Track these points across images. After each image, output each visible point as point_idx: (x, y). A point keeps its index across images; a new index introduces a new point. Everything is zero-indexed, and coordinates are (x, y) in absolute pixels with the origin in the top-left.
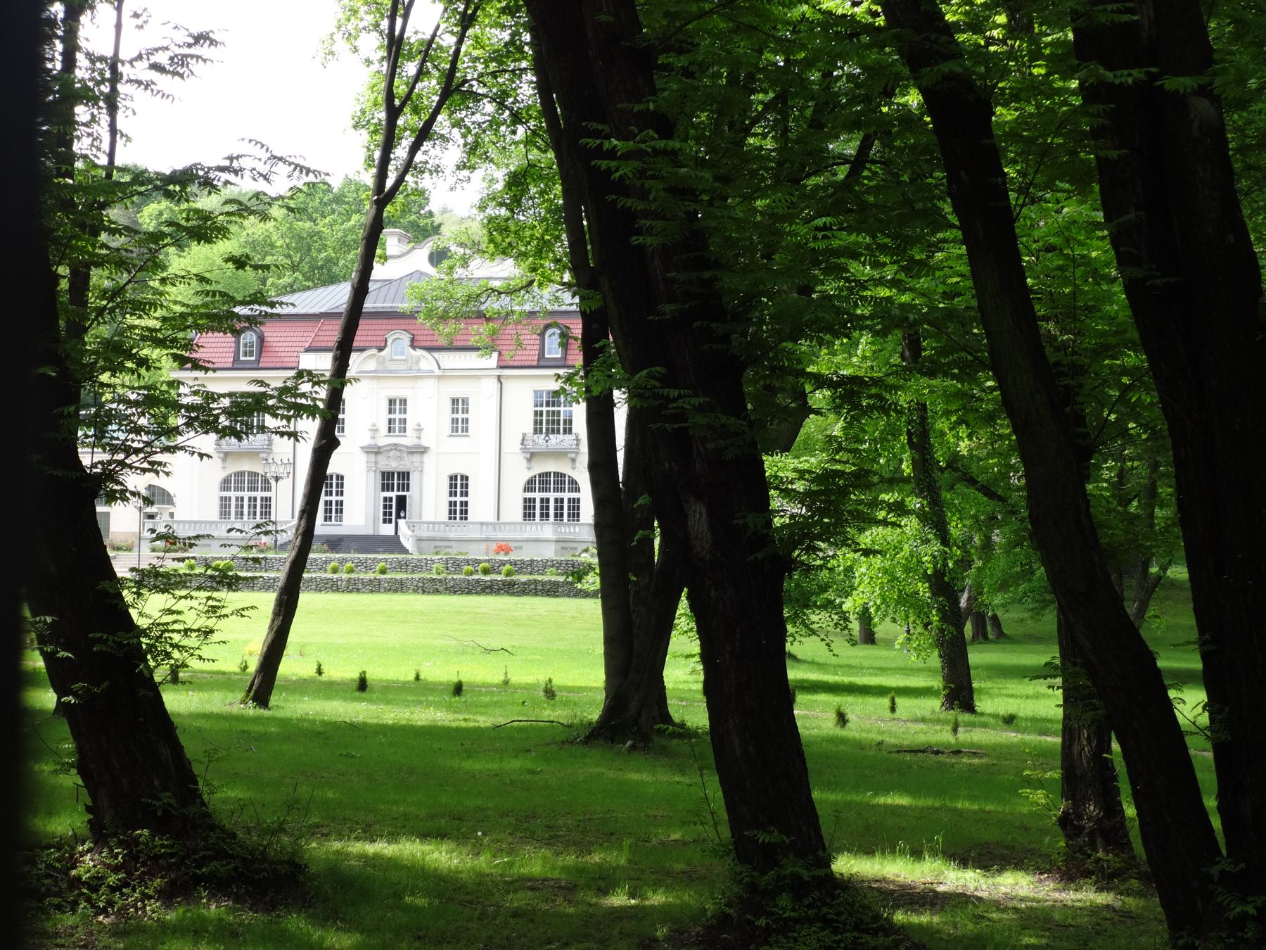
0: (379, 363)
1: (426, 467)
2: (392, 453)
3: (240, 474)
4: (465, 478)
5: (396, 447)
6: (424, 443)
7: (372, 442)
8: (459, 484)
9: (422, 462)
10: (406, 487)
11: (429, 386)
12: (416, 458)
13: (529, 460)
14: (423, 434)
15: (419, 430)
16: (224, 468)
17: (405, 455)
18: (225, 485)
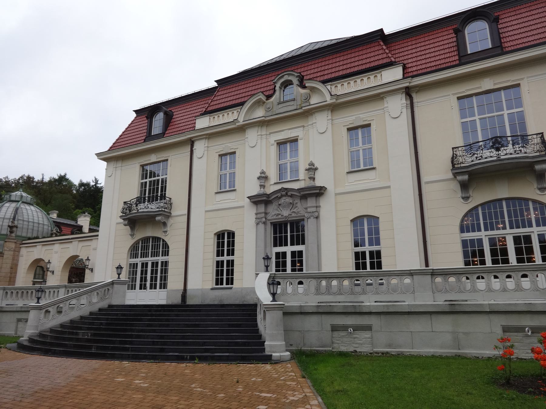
0: (268, 110)
1: (323, 212)
2: (282, 201)
3: (145, 240)
4: (373, 220)
5: (285, 192)
6: (318, 183)
7: (262, 191)
8: (366, 228)
9: (318, 207)
10: (300, 239)
11: (322, 121)
12: (311, 202)
13: (464, 186)
14: (318, 175)
15: (312, 169)
16: (132, 235)
17: (297, 201)
18: (134, 251)
